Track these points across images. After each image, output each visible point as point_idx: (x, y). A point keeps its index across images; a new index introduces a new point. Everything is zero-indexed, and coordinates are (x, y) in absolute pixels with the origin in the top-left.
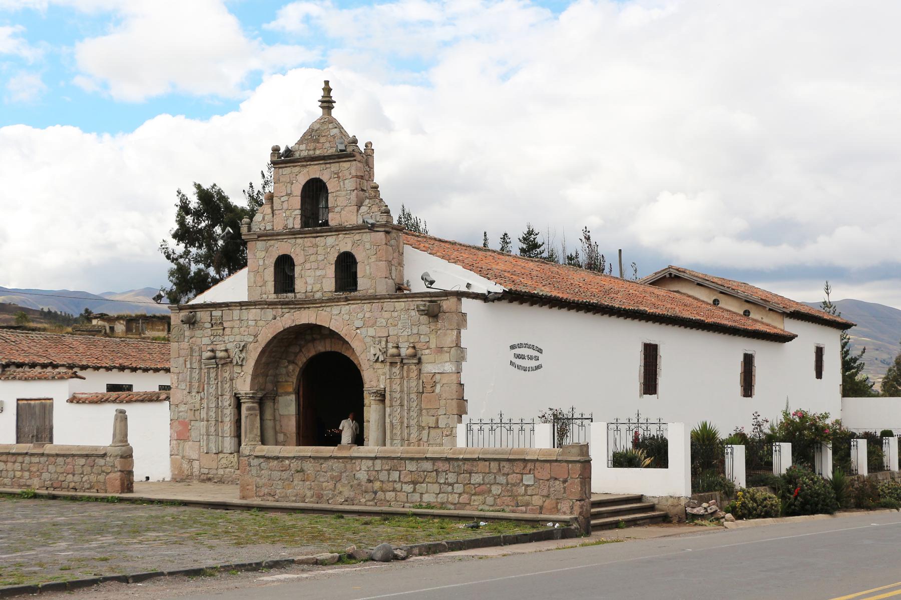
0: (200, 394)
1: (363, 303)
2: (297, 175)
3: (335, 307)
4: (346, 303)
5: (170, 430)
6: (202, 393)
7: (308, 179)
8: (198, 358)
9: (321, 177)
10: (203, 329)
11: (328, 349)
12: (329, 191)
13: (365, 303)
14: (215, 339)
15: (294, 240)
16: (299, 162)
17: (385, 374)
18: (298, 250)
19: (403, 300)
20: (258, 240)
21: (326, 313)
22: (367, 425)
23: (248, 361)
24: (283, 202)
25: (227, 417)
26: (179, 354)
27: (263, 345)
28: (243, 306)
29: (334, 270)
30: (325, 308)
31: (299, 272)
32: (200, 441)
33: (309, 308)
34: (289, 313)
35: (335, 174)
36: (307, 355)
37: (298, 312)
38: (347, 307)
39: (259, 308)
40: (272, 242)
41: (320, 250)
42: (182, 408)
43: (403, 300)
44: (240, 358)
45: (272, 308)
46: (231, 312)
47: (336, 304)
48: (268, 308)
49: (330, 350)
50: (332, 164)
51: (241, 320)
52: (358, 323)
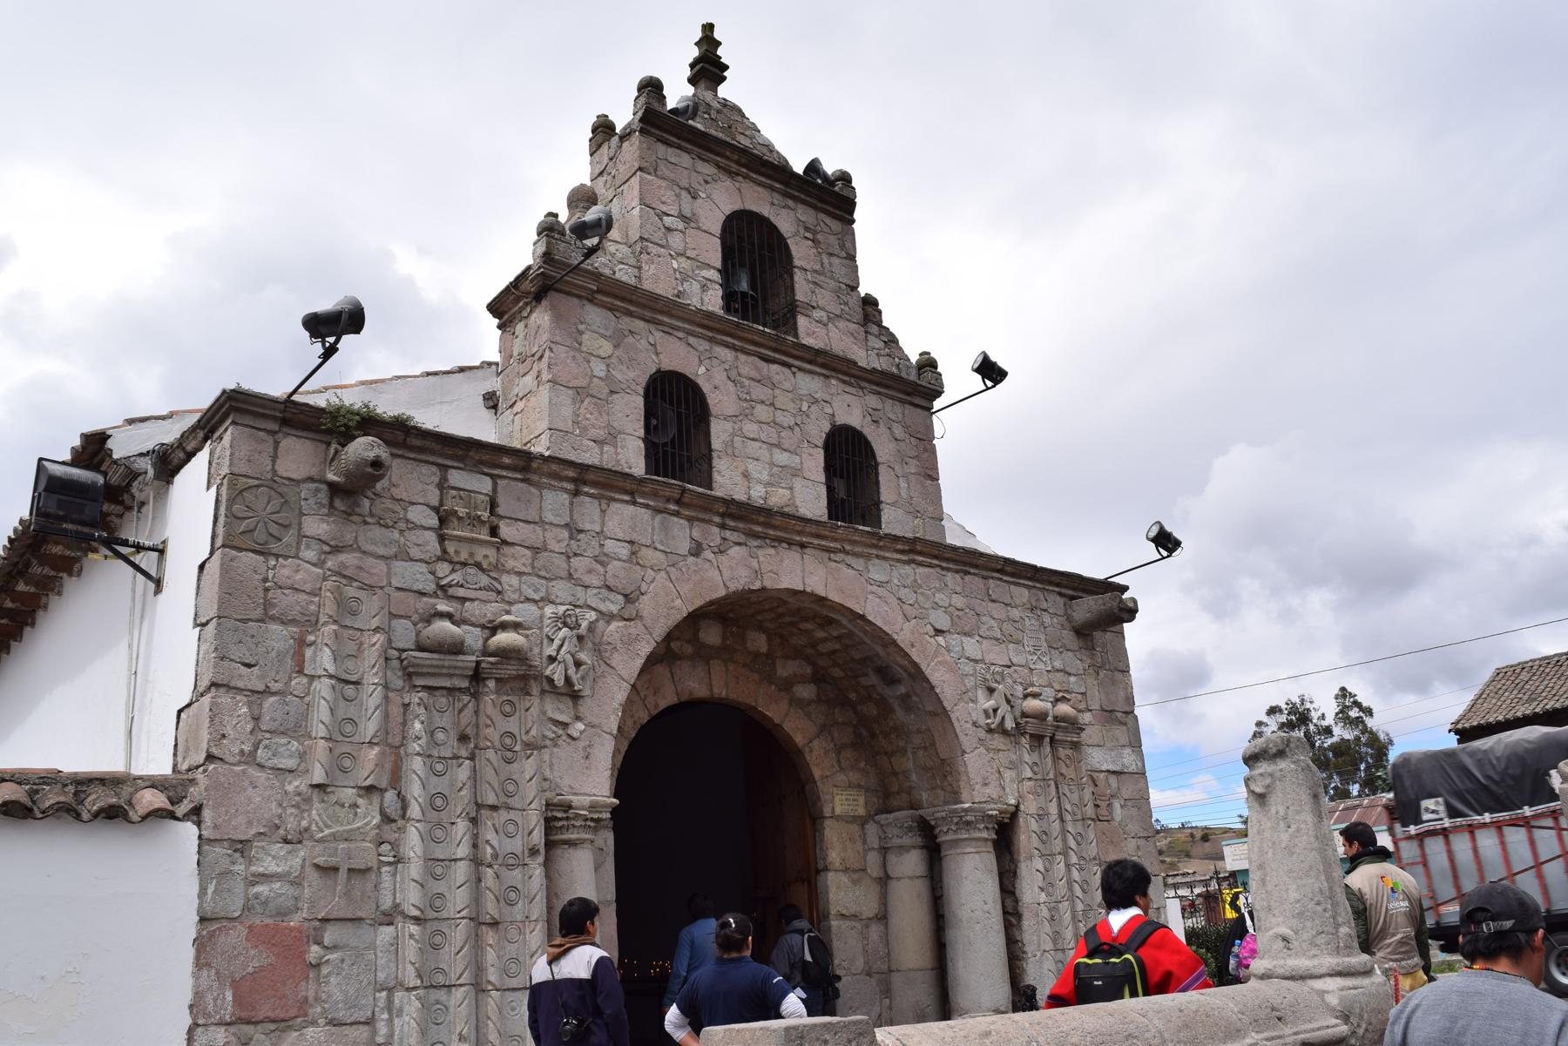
0: (376, 799)
1: (943, 568)
2: (707, 182)
3: (877, 561)
4: (905, 558)
5: (196, 976)
6: (390, 796)
7: (737, 206)
8: (379, 638)
9: (772, 219)
10: (402, 525)
11: (720, 691)
12: (797, 262)
13: (948, 569)
14: (457, 577)
15: (704, 345)
16: (717, 154)
17: (1013, 766)
18: (719, 377)
19: (1026, 583)
20: (591, 301)
21: (851, 572)
22: (839, 927)
23: (600, 683)
24: (669, 229)
25: (511, 904)
26: (267, 605)
27: (660, 631)
28: (585, 483)
29: (823, 465)
30: (850, 560)
31: (725, 437)
32: (370, 1022)
33: (803, 546)
34: (744, 548)
35: (807, 229)
36: (651, 700)
37: (772, 551)
38: (908, 569)
39: (647, 506)
40: (641, 324)
41: (783, 400)
42: (275, 858)
43: (1026, 583)
44: (578, 664)
45: (690, 519)
46: (533, 490)
47: (882, 553)
48: (677, 514)
49: (724, 694)
50: (800, 206)
51: (575, 531)
52: (943, 622)
